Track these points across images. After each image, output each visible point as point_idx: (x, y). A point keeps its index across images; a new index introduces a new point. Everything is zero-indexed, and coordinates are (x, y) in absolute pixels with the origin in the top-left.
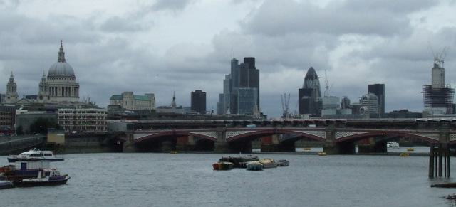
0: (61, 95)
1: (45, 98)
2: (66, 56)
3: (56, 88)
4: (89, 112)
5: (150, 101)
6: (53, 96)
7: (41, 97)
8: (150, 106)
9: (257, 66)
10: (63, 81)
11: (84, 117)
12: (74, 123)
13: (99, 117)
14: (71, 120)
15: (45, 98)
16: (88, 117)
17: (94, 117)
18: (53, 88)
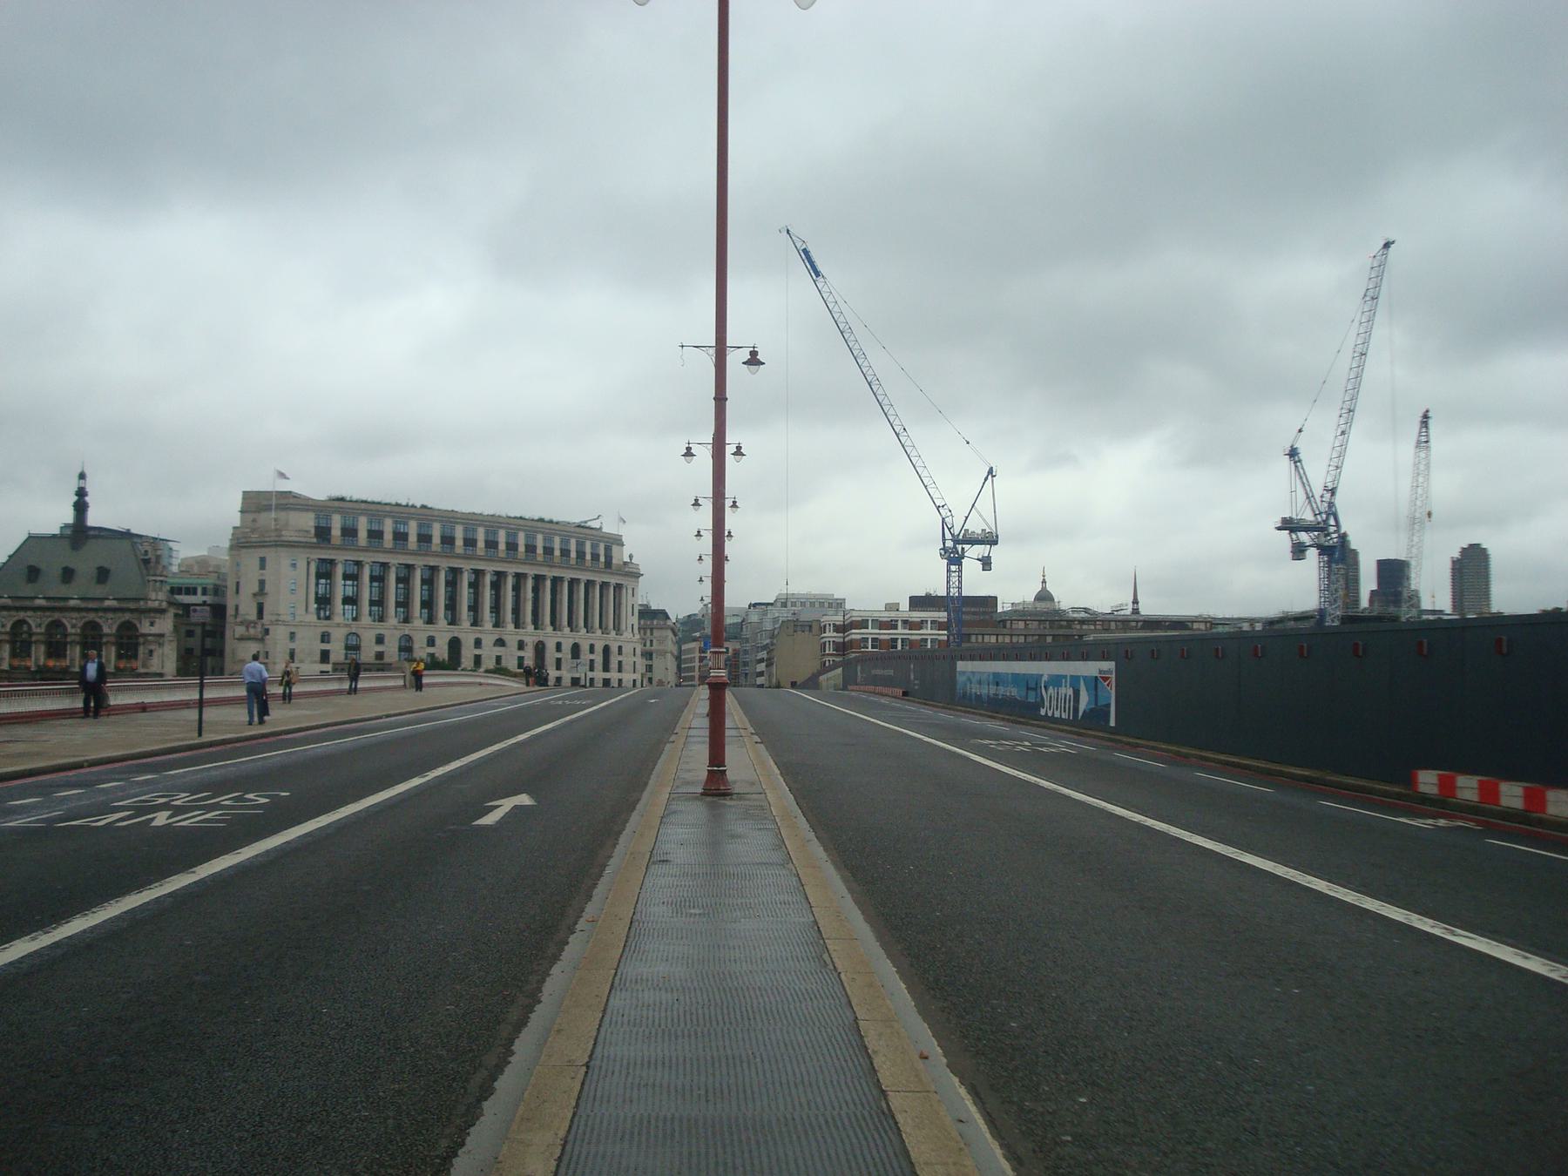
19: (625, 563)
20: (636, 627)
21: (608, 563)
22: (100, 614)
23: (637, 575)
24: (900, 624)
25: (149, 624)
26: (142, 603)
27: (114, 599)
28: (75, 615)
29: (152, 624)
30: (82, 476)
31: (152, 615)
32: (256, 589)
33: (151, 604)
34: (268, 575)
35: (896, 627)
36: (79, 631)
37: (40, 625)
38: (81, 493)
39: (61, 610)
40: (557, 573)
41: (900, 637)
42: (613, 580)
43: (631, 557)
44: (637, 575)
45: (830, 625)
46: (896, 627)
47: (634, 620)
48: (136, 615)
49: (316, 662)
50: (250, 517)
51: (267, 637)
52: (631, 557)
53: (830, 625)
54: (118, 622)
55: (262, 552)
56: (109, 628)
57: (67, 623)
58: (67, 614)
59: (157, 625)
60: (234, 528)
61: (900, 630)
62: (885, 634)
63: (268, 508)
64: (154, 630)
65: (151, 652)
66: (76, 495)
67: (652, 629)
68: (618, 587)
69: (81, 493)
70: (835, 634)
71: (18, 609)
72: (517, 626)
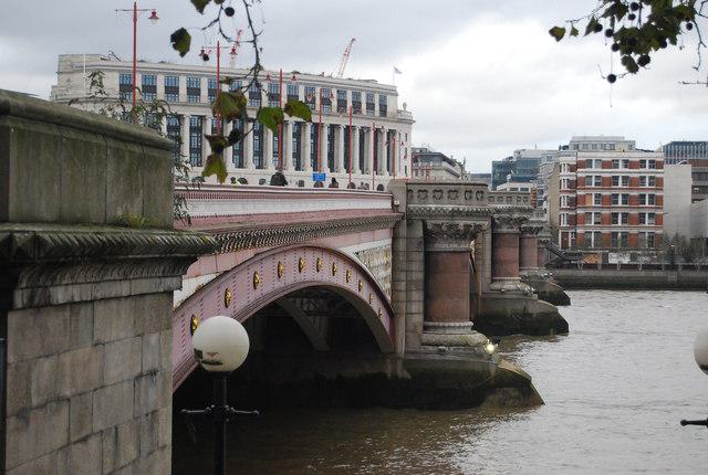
19: (399, 112)
20: (409, 169)
21: (383, 111)
23: (410, 122)
24: (621, 163)
35: (617, 166)
40: (334, 121)
41: (621, 175)
42: (387, 127)
43: (405, 105)
44: (410, 122)
46: (617, 166)
47: (408, 162)
50: (65, 77)
52: (405, 105)
60: (53, 87)
61: (621, 168)
62: (607, 173)
67: (428, 171)
68: (391, 133)
72: (298, 168)
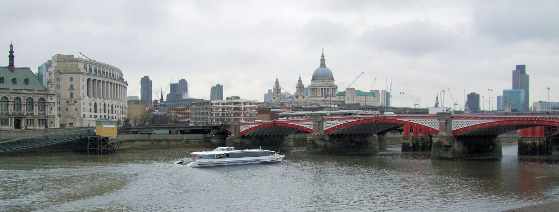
0: (320, 95)
1: (300, 97)
2: (326, 63)
3: (317, 89)
4: (234, 103)
5: (375, 97)
6: (314, 96)
7: (297, 97)
8: (375, 101)
9: (527, 72)
10: (322, 83)
11: (231, 109)
12: (223, 115)
13: (245, 109)
14: (220, 113)
15: (300, 97)
16: (235, 108)
17: (239, 109)
18: (314, 89)
22: (33, 95)
23: (127, 85)
25: (50, 99)
26: (47, 92)
27: (37, 90)
28: (24, 95)
29: (51, 99)
30: (11, 46)
31: (51, 96)
32: (69, 87)
33: (51, 92)
34: (73, 83)
36: (25, 101)
37: (24, 99)
38: (11, 52)
39: (19, 93)
45: (220, 103)
48: (45, 96)
49: (88, 112)
51: (76, 103)
53: (220, 103)
54: (39, 98)
55: (71, 75)
56: (36, 99)
57: (21, 98)
58: (21, 95)
59: (53, 99)
63: (70, 61)
64: (52, 101)
65: (51, 108)
66: (9, 53)
69: (11, 52)
70: (221, 105)
71: (16, 93)
